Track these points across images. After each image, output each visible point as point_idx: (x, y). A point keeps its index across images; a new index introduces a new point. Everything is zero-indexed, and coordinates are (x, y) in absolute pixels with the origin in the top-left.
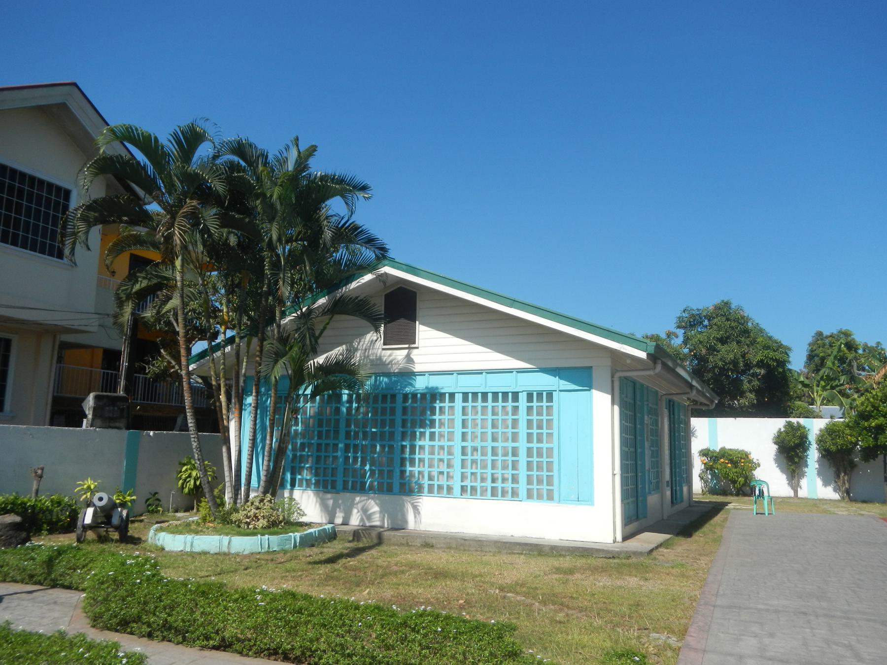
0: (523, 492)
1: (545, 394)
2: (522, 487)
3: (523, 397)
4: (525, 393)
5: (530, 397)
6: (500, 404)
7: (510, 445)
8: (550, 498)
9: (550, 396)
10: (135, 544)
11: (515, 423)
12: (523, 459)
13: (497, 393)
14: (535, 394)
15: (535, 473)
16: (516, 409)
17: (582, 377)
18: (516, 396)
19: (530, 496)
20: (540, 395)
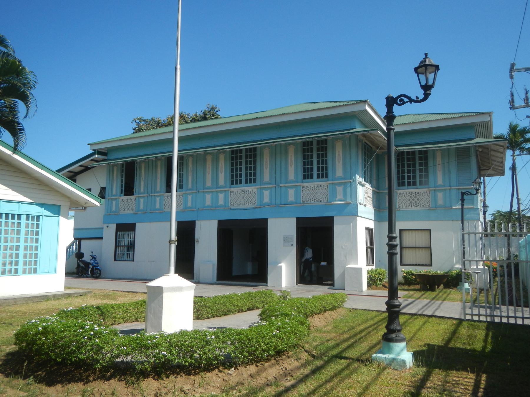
0: (20, 270)
1: (36, 217)
2: (21, 267)
3: (23, 218)
4: (25, 216)
5: (27, 218)
6: (10, 221)
7: (15, 244)
8: (35, 271)
9: (38, 218)
10: (64, 311)
11: (19, 232)
12: (21, 252)
13: (9, 214)
14: (30, 216)
15: (28, 259)
16: (19, 224)
17: (56, 210)
18: (19, 216)
19: (24, 272)
20: (33, 217)
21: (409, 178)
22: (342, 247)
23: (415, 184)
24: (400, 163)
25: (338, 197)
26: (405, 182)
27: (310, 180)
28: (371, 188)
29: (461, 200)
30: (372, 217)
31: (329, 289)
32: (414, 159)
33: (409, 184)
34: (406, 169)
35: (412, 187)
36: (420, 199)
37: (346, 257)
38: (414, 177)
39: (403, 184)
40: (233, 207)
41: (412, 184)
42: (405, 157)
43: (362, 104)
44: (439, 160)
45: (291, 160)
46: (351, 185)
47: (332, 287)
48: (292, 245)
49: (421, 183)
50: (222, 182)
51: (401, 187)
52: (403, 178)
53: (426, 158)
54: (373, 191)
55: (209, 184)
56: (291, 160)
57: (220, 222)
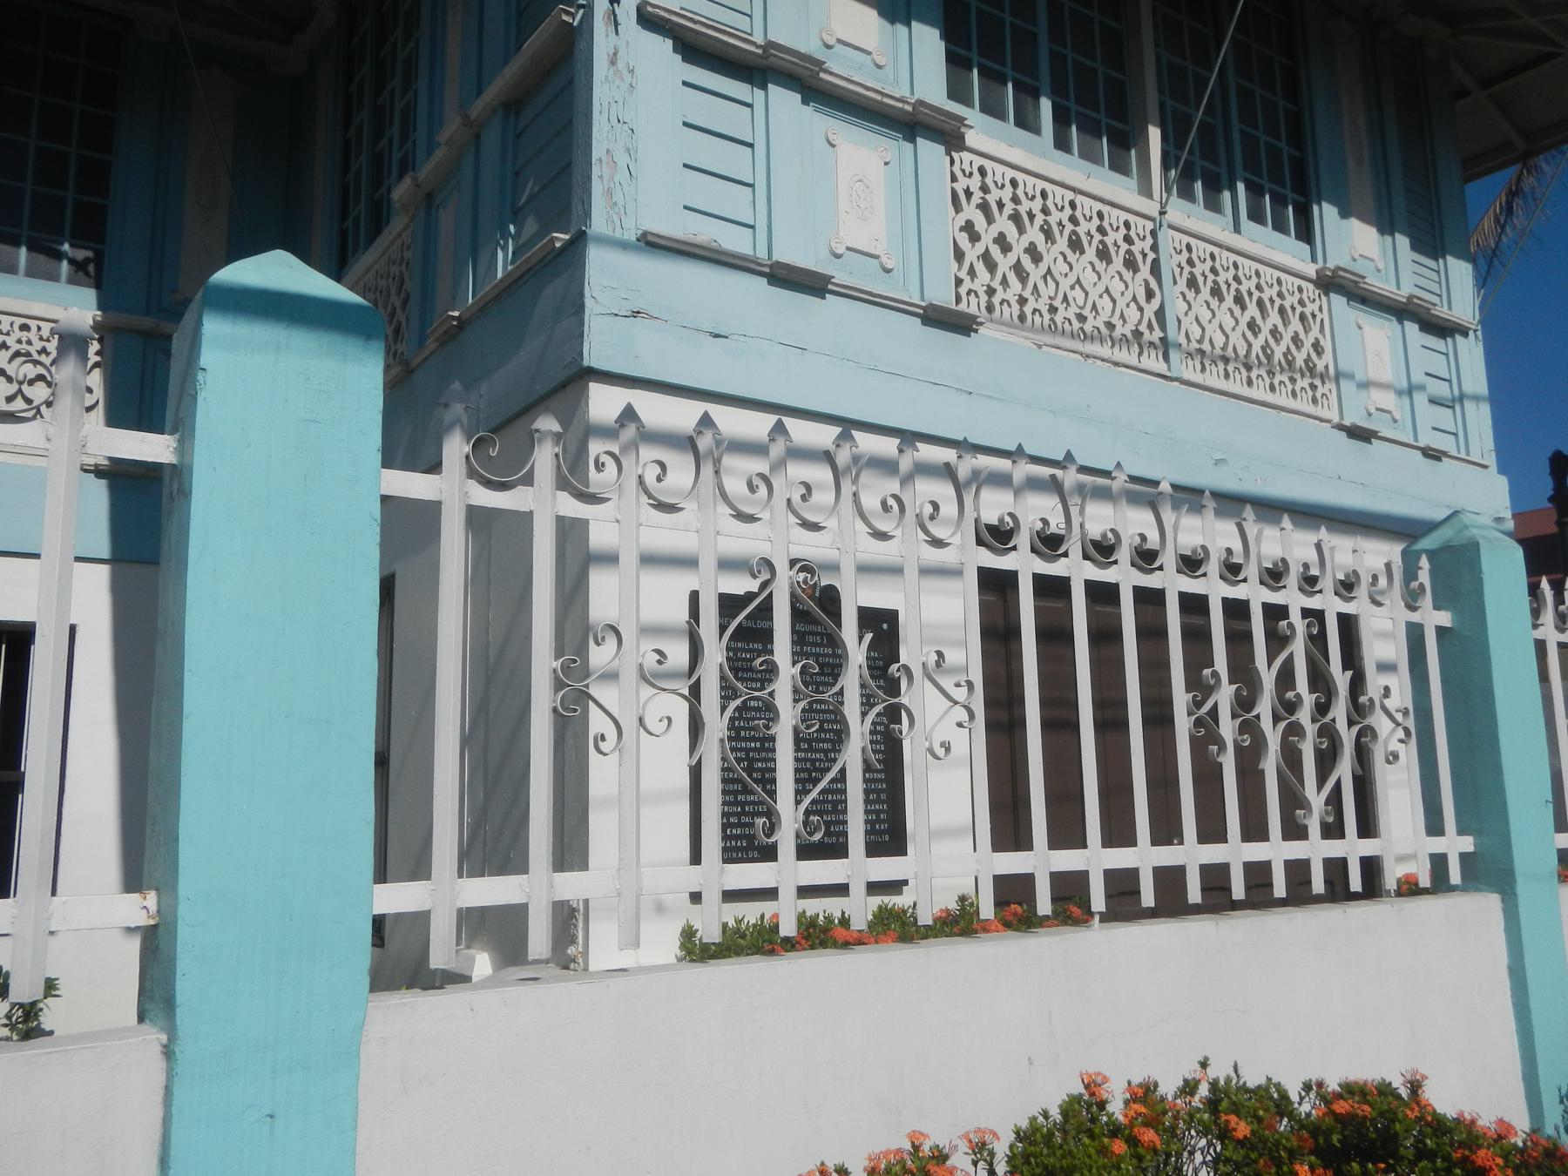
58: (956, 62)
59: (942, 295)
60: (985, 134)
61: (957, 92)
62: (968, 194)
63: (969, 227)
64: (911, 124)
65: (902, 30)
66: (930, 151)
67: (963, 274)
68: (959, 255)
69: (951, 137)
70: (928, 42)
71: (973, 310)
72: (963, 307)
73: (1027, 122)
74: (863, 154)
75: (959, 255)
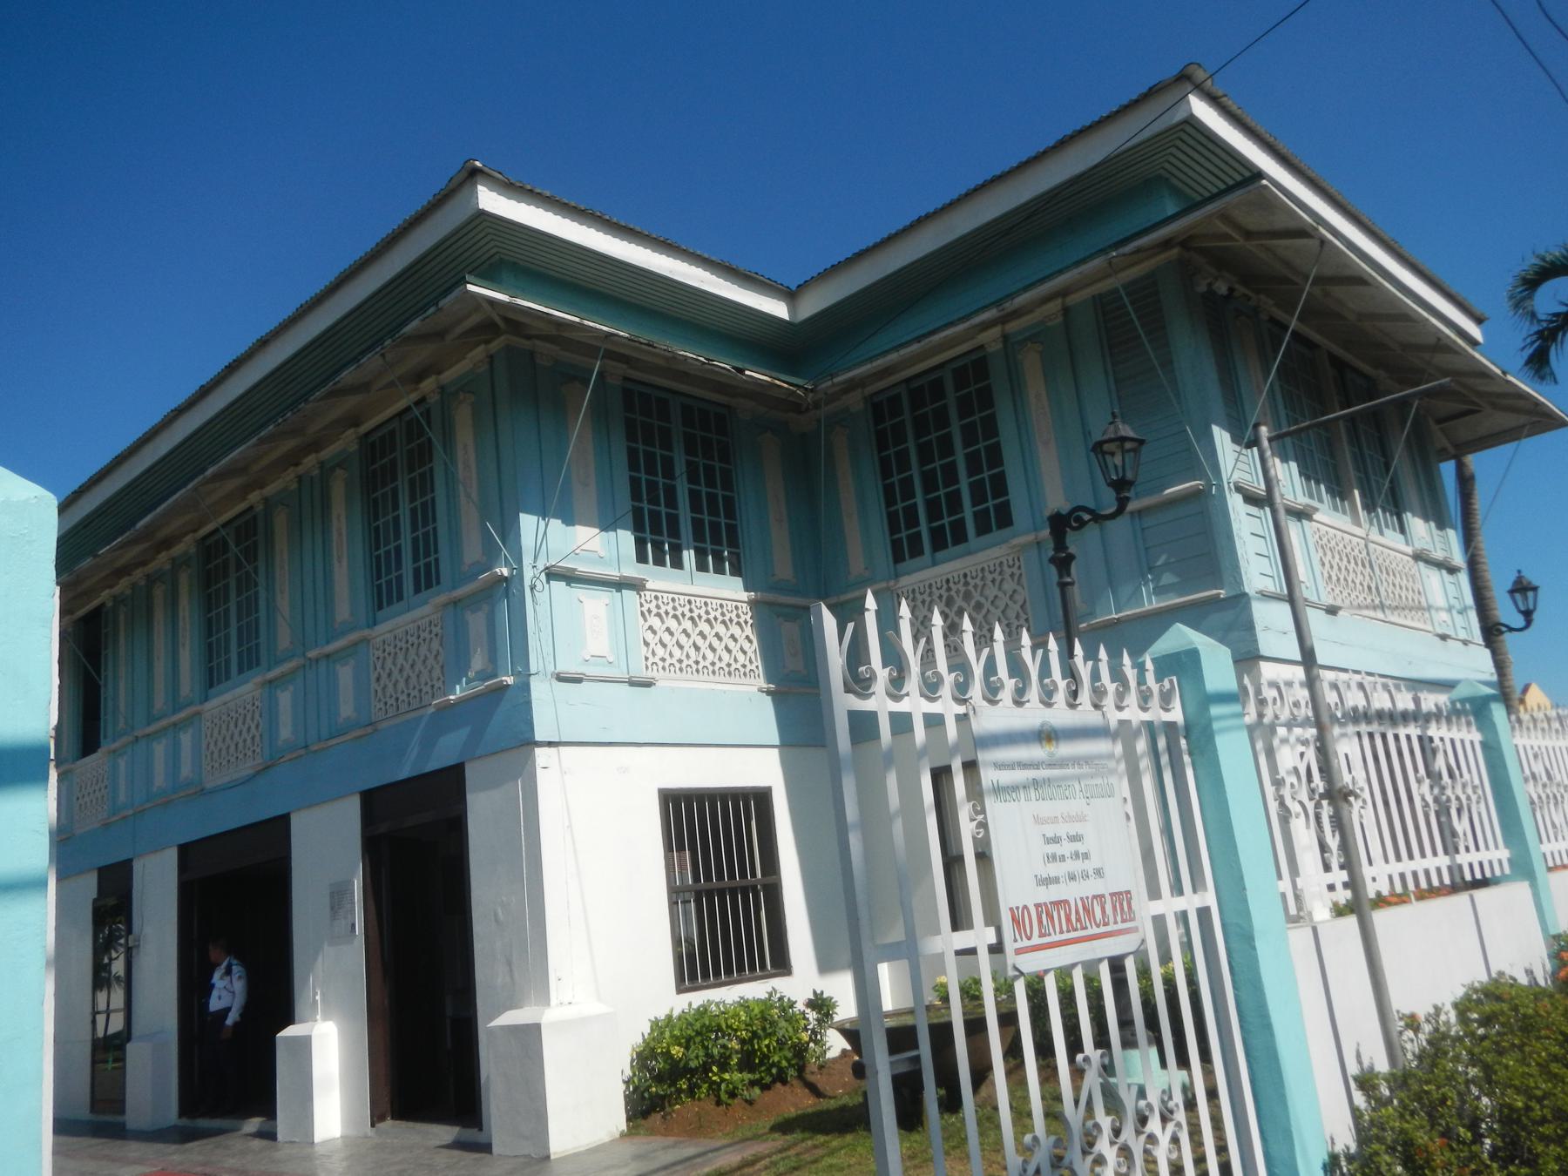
21: (934, 511)
22: (496, 915)
23: (960, 536)
24: (891, 451)
25: (478, 662)
26: (919, 534)
27: (396, 607)
28: (744, 596)
29: (1052, 560)
30: (770, 731)
31: (459, 1145)
32: (942, 419)
33: (939, 543)
34: (915, 473)
35: (952, 550)
36: (987, 605)
37: (509, 964)
38: (955, 502)
39: (916, 551)
40: (208, 786)
41: (948, 538)
42: (907, 416)
43: (465, 190)
44: (1035, 387)
45: (340, 534)
46: (507, 594)
47: (470, 1134)
48: (353, 925)
49: (983, 528)
50: (185, 688)
51: (909, 563)
52: (912, 521)
53: (986, 398)
54: (752, 604)
55: (160, 702)
56: (340, 534)
57: (185, 851)
58: (640, 544)
59: (640, 672)
60: (660, 579)
61: (641, 558)
62: (649, 611)
63: (650, 628)
64: (620, 585)
65: (612, 534)
66: (629, 595)
67: (650, 655)
68: (647, 644)
69: (637, 586)
70: (626, 539)
71: (655, 674)
72: (649, 674)
73: (678, 564)
74: (596, 603)
75: (647, 644)
